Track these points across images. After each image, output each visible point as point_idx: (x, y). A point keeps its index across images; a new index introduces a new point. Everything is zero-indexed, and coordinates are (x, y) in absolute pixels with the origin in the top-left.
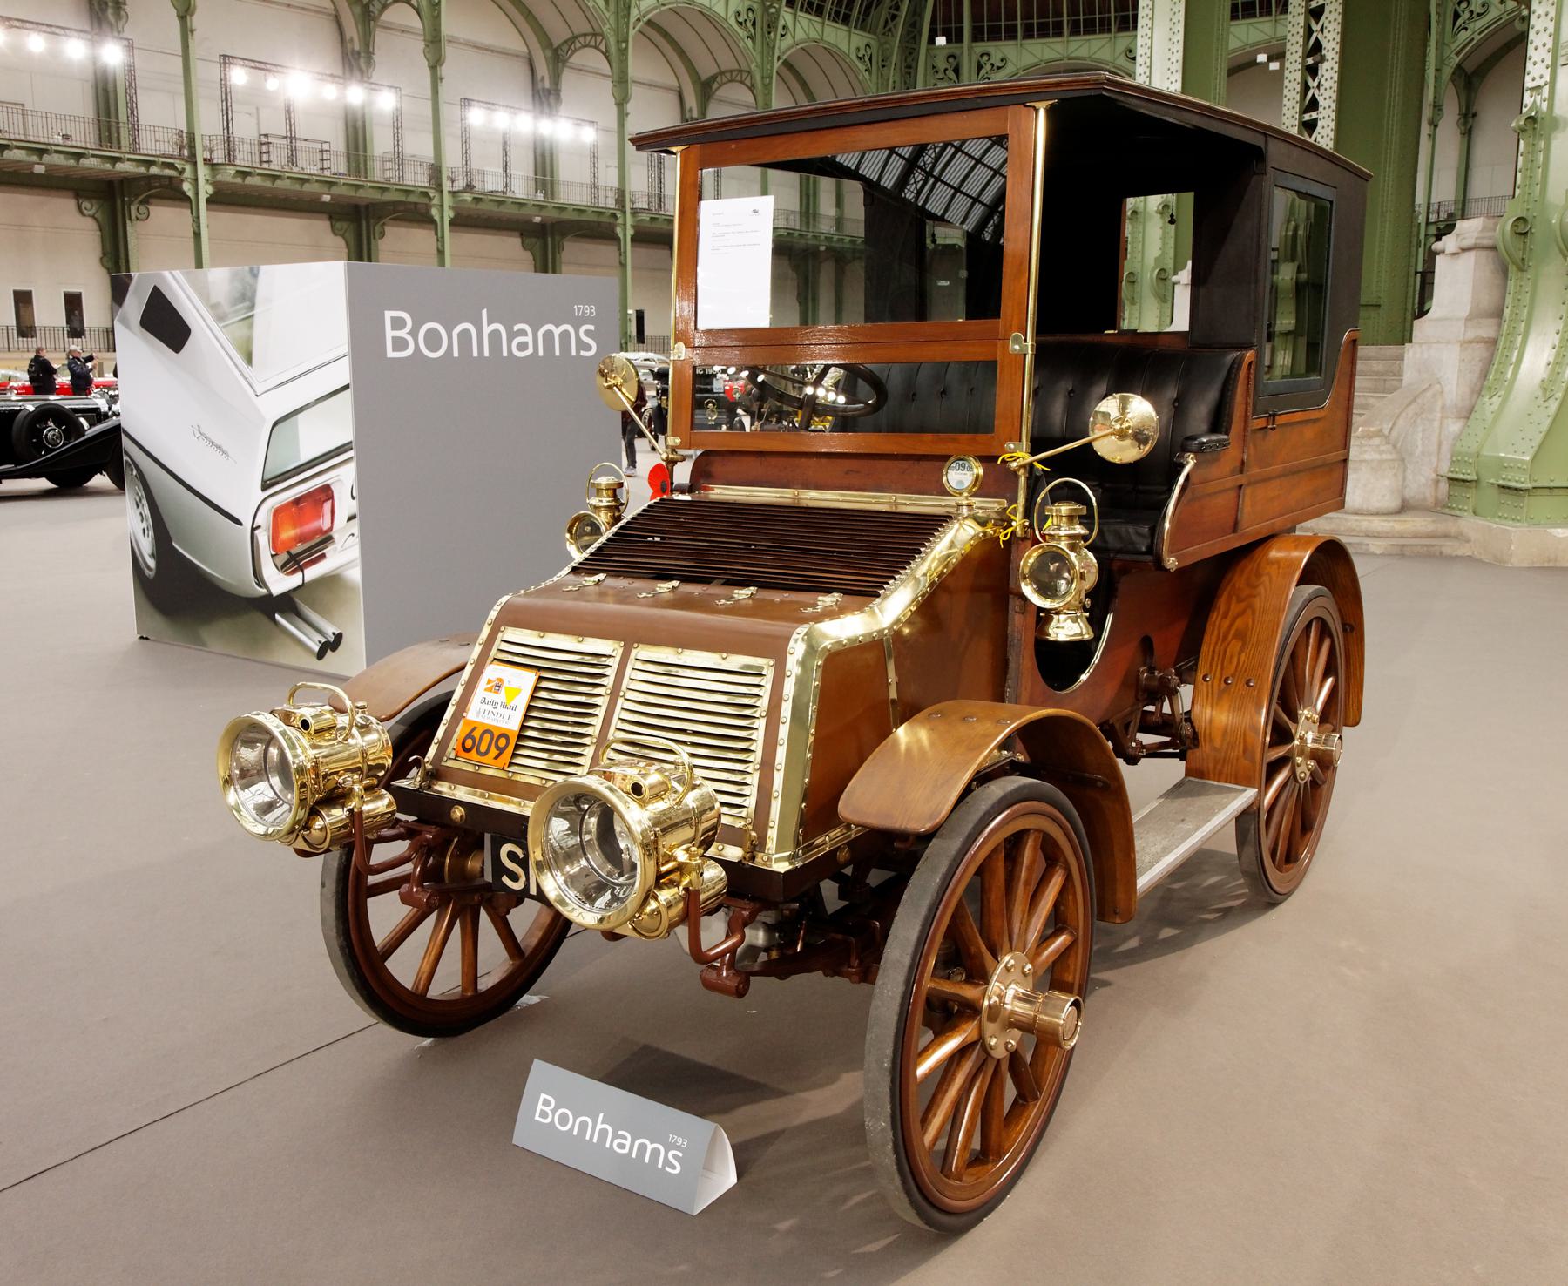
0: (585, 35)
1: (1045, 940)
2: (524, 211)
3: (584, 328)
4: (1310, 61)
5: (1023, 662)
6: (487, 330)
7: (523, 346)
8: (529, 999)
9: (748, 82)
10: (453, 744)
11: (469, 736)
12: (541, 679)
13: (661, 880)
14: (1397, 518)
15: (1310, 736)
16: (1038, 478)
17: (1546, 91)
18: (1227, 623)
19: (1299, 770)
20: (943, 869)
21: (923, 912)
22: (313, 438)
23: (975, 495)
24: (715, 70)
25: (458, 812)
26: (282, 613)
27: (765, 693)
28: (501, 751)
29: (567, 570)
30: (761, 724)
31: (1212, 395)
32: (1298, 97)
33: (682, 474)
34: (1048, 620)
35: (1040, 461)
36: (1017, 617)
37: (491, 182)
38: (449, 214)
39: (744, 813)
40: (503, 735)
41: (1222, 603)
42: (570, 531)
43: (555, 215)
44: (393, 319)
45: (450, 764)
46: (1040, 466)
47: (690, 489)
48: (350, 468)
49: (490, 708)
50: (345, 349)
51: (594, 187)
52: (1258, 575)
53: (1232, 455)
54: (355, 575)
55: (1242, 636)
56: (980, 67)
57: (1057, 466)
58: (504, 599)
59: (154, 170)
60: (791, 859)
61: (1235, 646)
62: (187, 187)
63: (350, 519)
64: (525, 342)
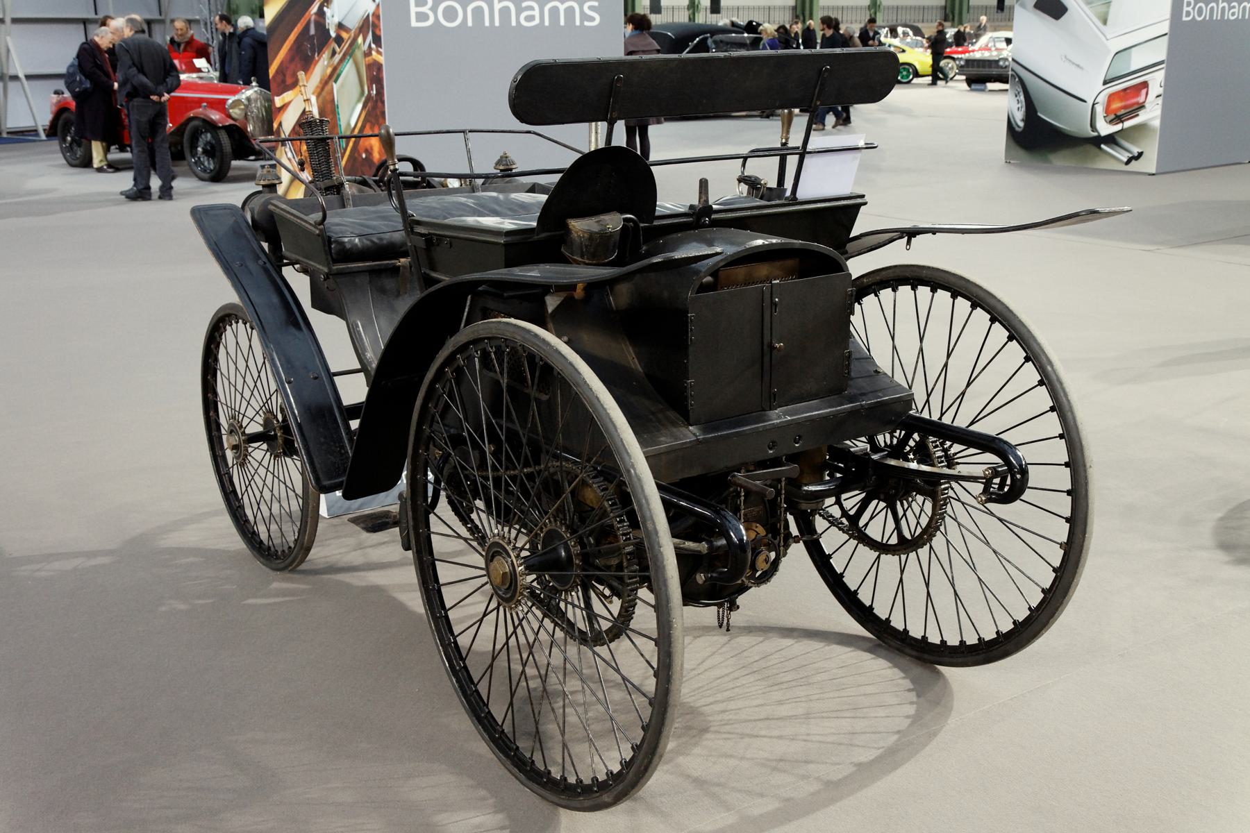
7: (1233, 14)
22: (1138, 60)
48: (1163, 72)
50: (1168, 16)
54: (1157, 123)
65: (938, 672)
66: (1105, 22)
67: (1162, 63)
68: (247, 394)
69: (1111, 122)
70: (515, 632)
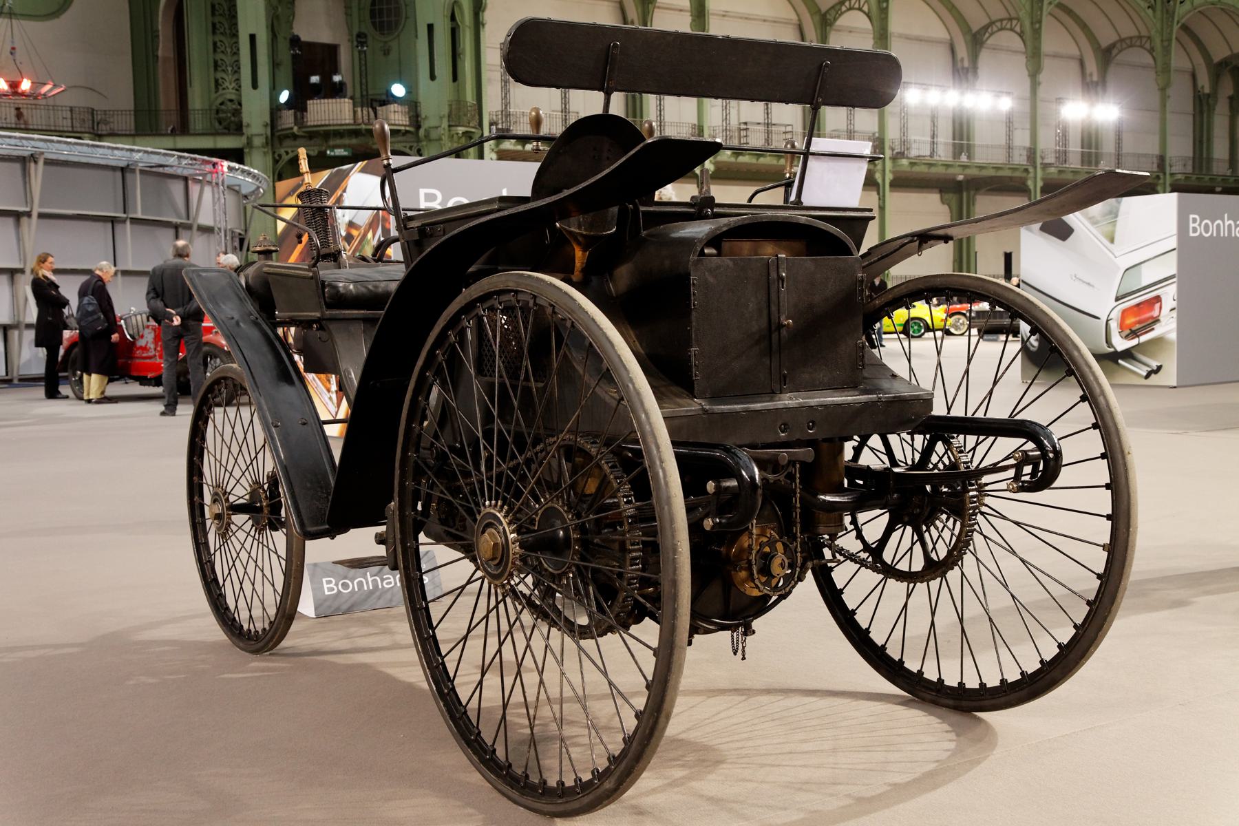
0: (1001, 20)
2: (951, 171)
6: (1227, 223)
22: (1149, 275)
24: (1114, 38)
26: (1123, 359)
37: (919, 148)
38: (889, 177)
43: (974, 172)
48: (1174, 287)
51: (1009, 148)
54: (1173, 336)
65: (979, 719)
66: (1112, 241)
67: (1173, 277)
68: (235, 449)
69: (1126, 337)
70: (497, 607)
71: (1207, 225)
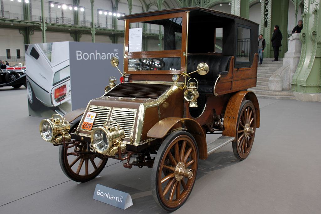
1: (187, 161)
2: (110, 32)
3: (116, 54)
4: (266, 2)
5: (187, 112)
6: (97, 54)
7: (104, 57)
8: (98, 177)
9: (157, 5)
10: (82, 126)
11: (85, 125)
12: (97, 114)
13: (113, 145)
14: (282, 92)
15: (247, 129)
16: (188, 78)
17: (308, 8)
18: (230, 107)
19: (245, 135)
20: (165, 145)
21: (162, 152)
23: (178, 81)
24: (150, 3)
25: (82, 138)
27: (135, 115)
28: (90, 127)
29: (104, 95)
30: (134, 121)
31: (226, 64)
32: (264, 9)
33: (126, 79)
34: (190, 104)
35: (189, 75)
36: (185, 104)
37: (103, 26)
38: (95, 32)
39: (131, 136)
40: (90, 124)
41: (229, 103)
42: (106, 89)
43: (116, 32)
44: (78, 52)
45: (81, 130)
46: (188, 76)
47: (128, 82)
49: (88, 119)
50: (69, 58)
52: (236, 98)
53: (229, 75)
54: (70, 102)
55: (232, 109)
56: (204, 2)
57: (192, 75)
58: (91, 100)
59: (35, 24)
60: (139, 144)
61: (231, 111)
62: (41, 28)
63: (70, 91)
64: (104, 57)
66: (50, 61)
67: (69, 77)
71: (86, 55)
